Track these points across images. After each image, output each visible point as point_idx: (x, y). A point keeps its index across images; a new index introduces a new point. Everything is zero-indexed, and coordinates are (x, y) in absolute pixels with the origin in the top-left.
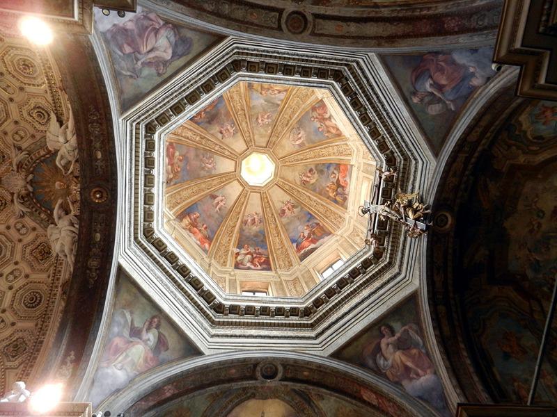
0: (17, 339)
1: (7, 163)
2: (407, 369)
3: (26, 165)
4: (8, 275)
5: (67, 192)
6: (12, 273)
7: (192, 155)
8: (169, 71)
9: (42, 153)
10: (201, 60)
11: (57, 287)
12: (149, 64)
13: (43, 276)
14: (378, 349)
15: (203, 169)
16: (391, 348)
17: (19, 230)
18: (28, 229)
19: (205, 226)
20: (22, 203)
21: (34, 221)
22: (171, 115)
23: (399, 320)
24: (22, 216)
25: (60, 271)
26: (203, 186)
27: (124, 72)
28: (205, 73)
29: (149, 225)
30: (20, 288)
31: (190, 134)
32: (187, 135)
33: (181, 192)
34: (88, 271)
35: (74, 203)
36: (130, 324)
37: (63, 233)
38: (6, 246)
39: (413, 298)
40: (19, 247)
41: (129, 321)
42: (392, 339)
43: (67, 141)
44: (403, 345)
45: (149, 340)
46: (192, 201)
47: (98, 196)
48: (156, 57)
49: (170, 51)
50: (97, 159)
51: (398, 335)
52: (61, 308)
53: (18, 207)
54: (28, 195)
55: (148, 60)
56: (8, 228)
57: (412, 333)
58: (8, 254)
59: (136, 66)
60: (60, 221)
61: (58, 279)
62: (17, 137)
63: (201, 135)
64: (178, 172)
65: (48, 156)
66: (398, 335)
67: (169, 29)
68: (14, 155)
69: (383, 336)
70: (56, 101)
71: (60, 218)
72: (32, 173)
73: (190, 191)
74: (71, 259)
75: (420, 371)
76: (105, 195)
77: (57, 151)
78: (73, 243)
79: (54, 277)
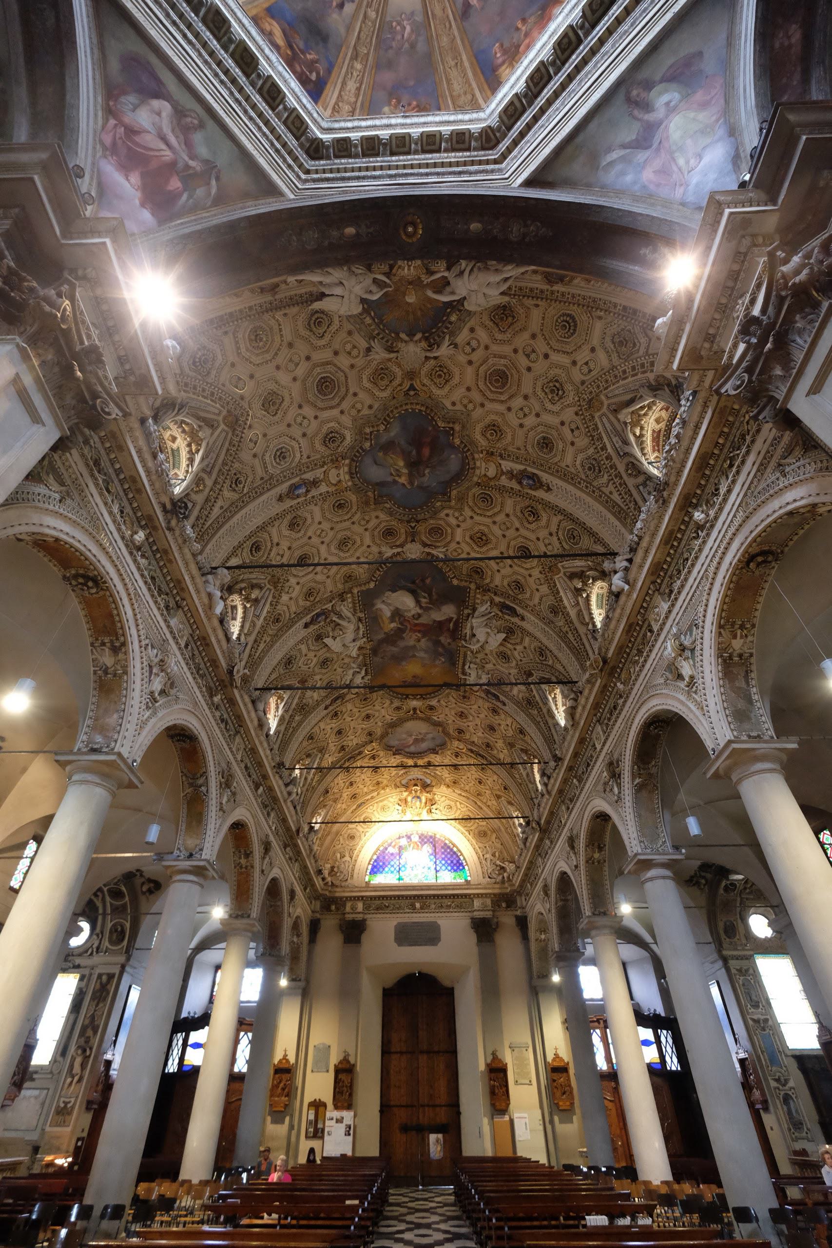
0: (613, 343)
1: (389, 364)
3: (387, 341)
4: (530, 361)
5: (416, 283)
6: (528, 356)
7: (388, 77)
8: (189, 103)
9: (368, 320)
10: (153, 33)
11: (552, 293)
12: (188, 145)
13: (536, 314)
15: (413, 46)
17: (473, 350)
18: (473, 338)
19: (520, 26)
20: (438, 346)
21: (460, 329)
22: (285, 108)
24: (456, 346)
25: (531, 290)
26: (445, 41)
27: (214, 191)
28: (182, 26)
29: (476, 140)
30: (548, 344)
31: (351, 86)
32: (353, 91)
33: (454, 94)
34: (527, 240)
35: (431, 273)
36: (628, 151)
37: (474, 287)
38: (494, 365)
40: (495, 348)
41: (622, 152)
43: (341, 283)
45: (667, 104)
46: (471, 64)
47: (410, 229)
48: (173, 131)
49: (156, 103)
50: (358, 234)
52: (583, 284)
53: (444, 350)
54: (427, 339)
55: (184, 147)
56: (470, 363)
58: (503, 361)
59: (198, 169)
60: (458, 291)
61: (542, 291)
62: (355, 352)
63: (352, 59)
64: (418, 106)
65: (372, 314)
67: (119, 106)
68: (377, 357)
70: (293, 302)
71: (453, 293)
72: (397, 334)
73: (454, 74)
74: (511, 271)
76: (410, 218)
77: (363, 301)
78: (487, 268)
79: (538, 298)
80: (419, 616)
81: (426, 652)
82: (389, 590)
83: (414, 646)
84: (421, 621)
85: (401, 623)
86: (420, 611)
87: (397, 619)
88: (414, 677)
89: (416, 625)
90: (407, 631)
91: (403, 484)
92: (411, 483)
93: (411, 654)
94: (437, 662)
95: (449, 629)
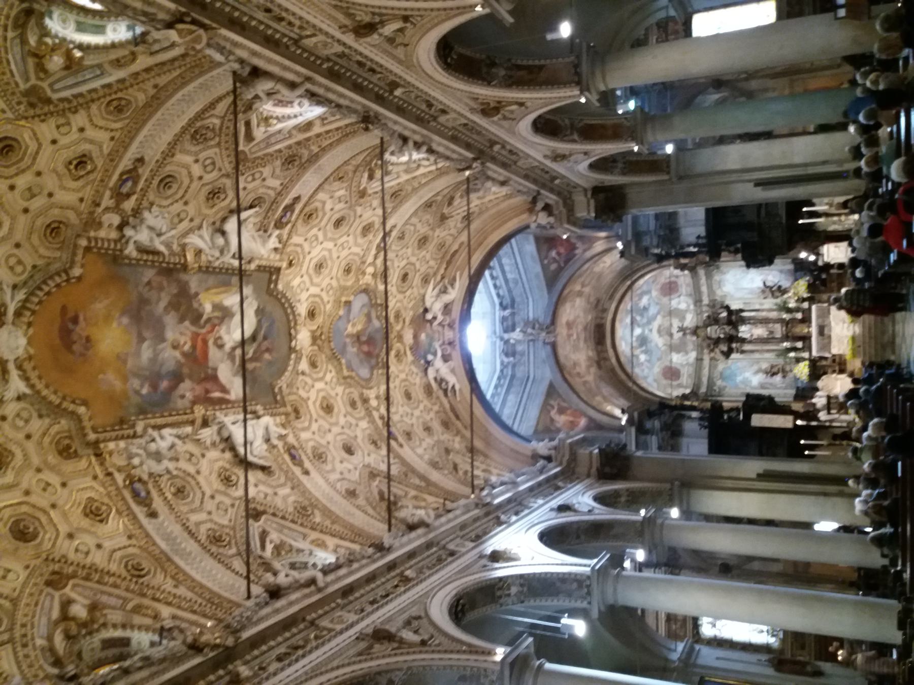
14: (552, 420)
44: (561, 411)
69: (549, 412)
80: (221, 347)
81: (154, 360)
82: (258, 307)
83: (163, 340)
84: (213, 352)
85: (209, 320)
86: (228, 347)
87: (216, 314)
88: (88, 339)
89: (205, 342)
90: (194, 329)
91: (346, 329)
92: (348, 336)
93: (147, 334)
94: (135, 383)
95: (207, 391)
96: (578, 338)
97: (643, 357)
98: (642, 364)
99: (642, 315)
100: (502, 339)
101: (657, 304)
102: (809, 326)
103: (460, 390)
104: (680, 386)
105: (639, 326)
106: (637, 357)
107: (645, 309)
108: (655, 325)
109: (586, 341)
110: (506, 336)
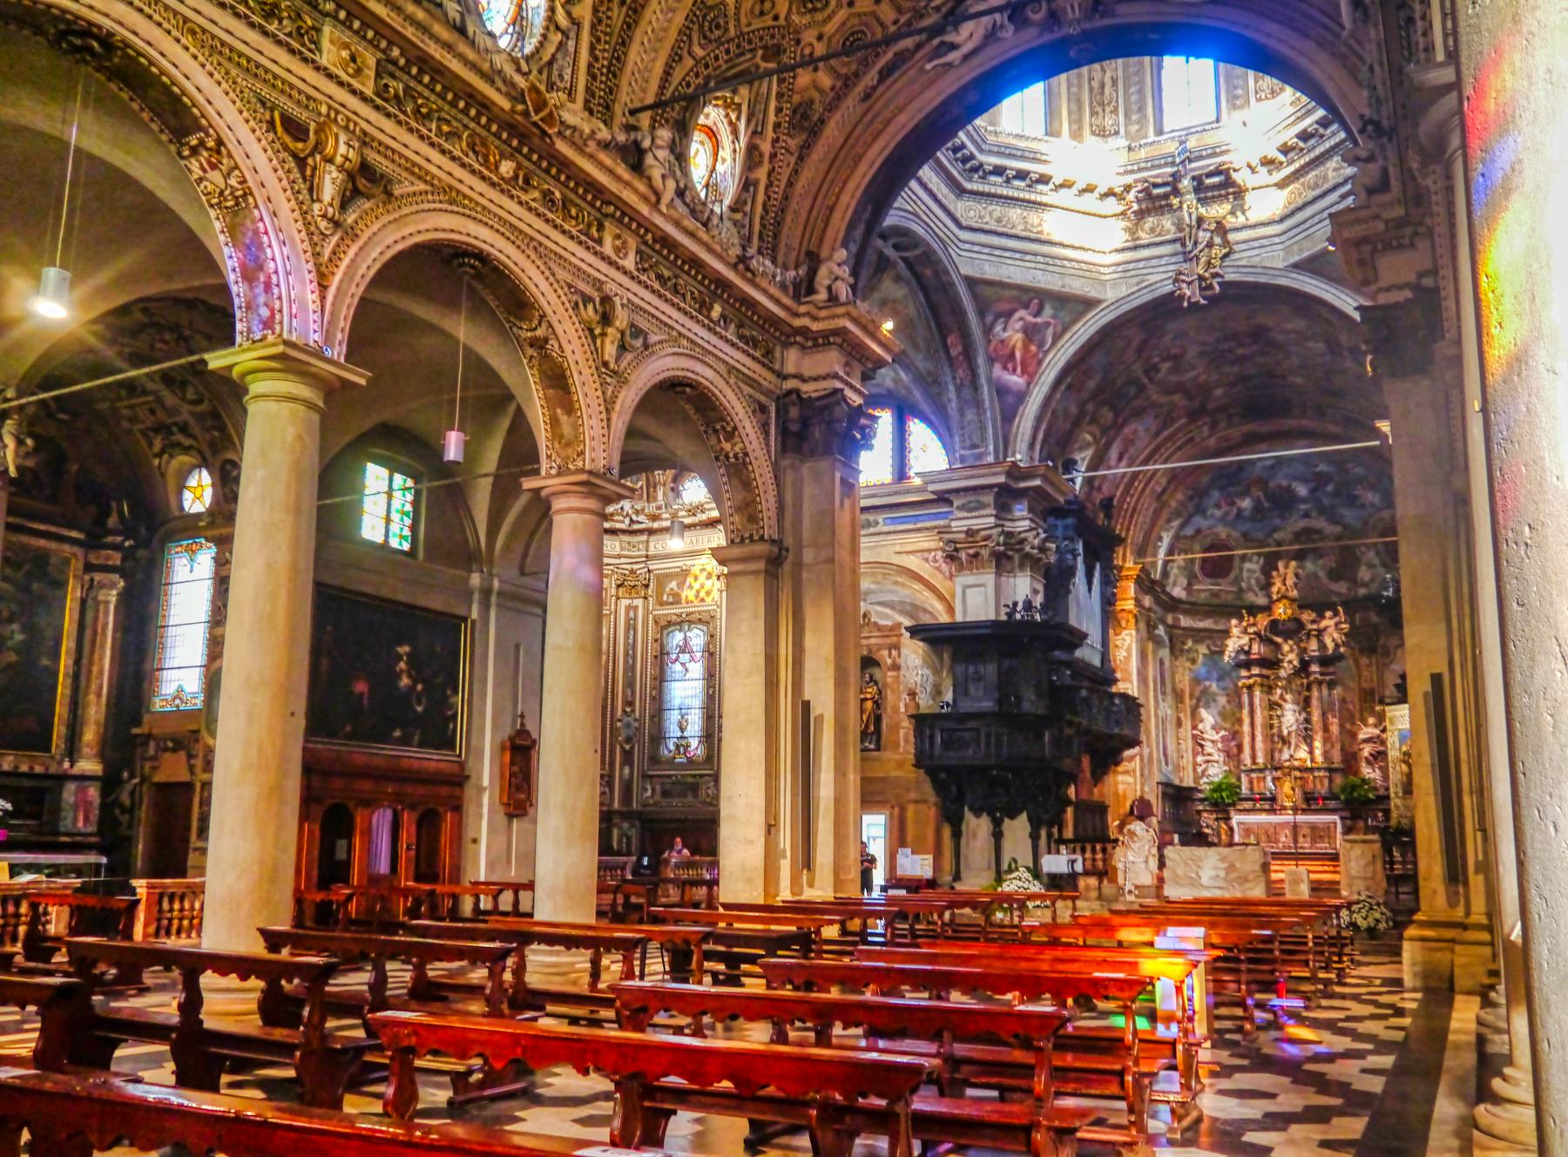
2: (1012, 356)
14: (1008, 315)
16: (1019, 325)
23: (1055, 308)
39: (1088, 304)
42: (1030, 319)
44: (1031, 332)
51: (1039, 320)
57: (1050, 332)
66: (1039, 320)
69: (1026, 307)
75: (1019, 369)
96: (1242, 359)
97: (1246, 504)
98: (1232, 504)
99: (1336, 494)
100: (1176, 177)
101: (1366, 523)
102: (1295, 810)
103: (949, 65)
104: (1192, 579)
105: (1313, 491)
106: (1245, 493)
107: (1352, 501)
108: (1320, 523)
109: (1244, 379)
110: (1186, 183)
